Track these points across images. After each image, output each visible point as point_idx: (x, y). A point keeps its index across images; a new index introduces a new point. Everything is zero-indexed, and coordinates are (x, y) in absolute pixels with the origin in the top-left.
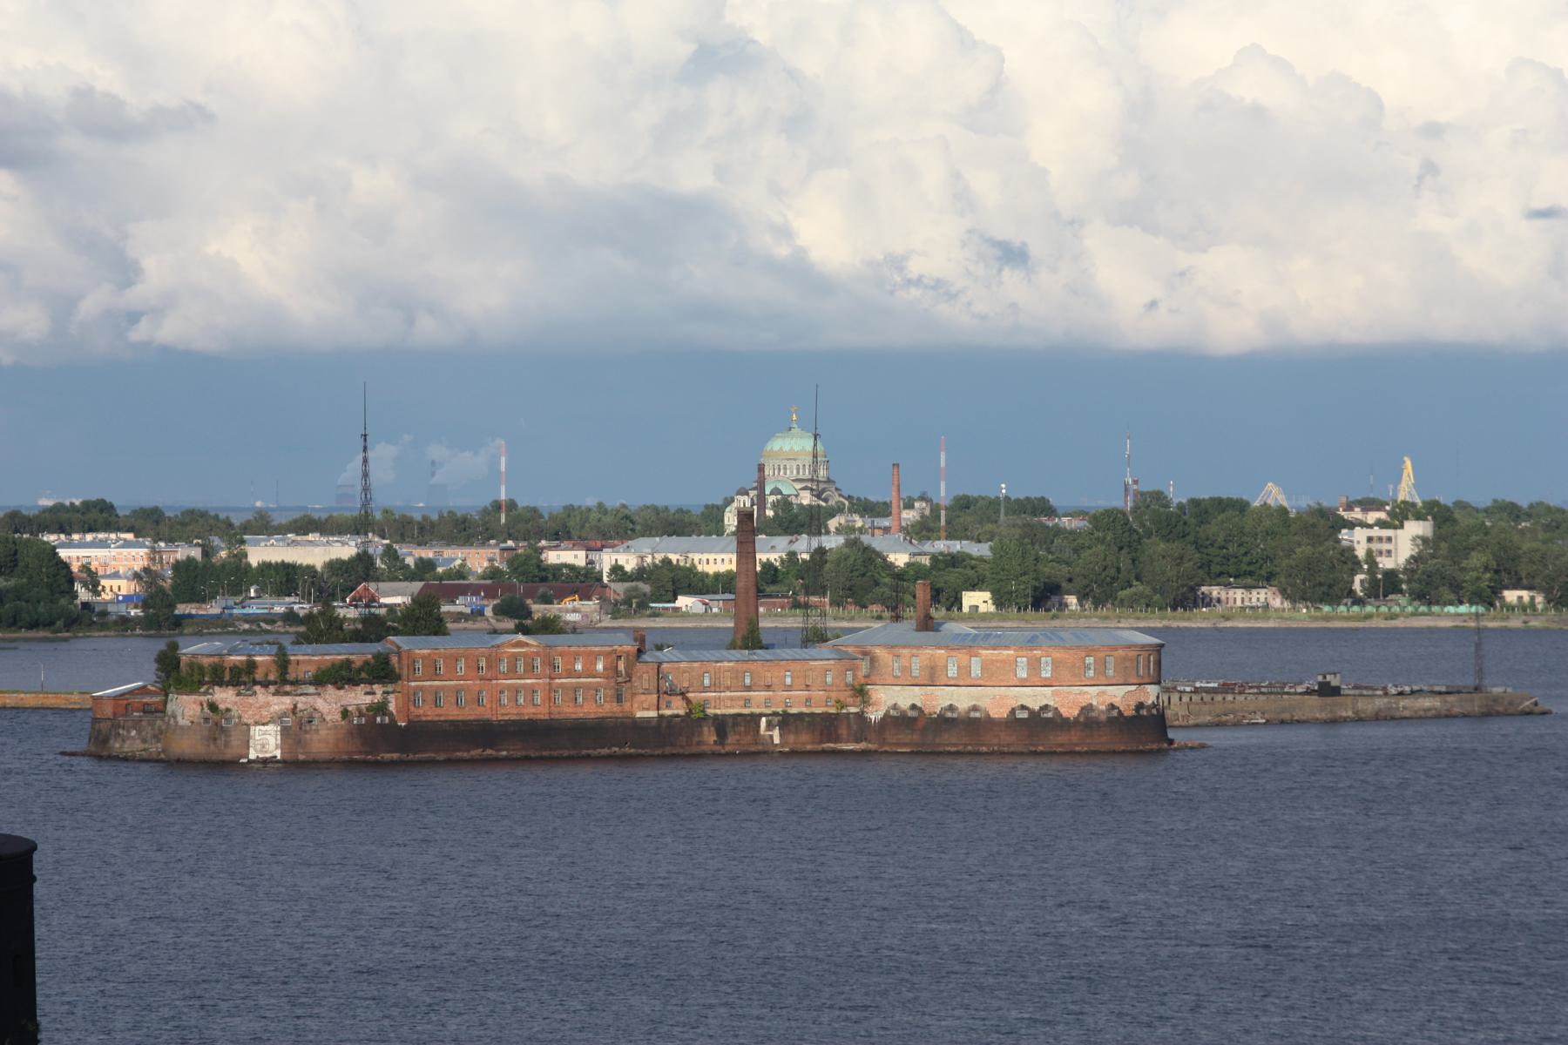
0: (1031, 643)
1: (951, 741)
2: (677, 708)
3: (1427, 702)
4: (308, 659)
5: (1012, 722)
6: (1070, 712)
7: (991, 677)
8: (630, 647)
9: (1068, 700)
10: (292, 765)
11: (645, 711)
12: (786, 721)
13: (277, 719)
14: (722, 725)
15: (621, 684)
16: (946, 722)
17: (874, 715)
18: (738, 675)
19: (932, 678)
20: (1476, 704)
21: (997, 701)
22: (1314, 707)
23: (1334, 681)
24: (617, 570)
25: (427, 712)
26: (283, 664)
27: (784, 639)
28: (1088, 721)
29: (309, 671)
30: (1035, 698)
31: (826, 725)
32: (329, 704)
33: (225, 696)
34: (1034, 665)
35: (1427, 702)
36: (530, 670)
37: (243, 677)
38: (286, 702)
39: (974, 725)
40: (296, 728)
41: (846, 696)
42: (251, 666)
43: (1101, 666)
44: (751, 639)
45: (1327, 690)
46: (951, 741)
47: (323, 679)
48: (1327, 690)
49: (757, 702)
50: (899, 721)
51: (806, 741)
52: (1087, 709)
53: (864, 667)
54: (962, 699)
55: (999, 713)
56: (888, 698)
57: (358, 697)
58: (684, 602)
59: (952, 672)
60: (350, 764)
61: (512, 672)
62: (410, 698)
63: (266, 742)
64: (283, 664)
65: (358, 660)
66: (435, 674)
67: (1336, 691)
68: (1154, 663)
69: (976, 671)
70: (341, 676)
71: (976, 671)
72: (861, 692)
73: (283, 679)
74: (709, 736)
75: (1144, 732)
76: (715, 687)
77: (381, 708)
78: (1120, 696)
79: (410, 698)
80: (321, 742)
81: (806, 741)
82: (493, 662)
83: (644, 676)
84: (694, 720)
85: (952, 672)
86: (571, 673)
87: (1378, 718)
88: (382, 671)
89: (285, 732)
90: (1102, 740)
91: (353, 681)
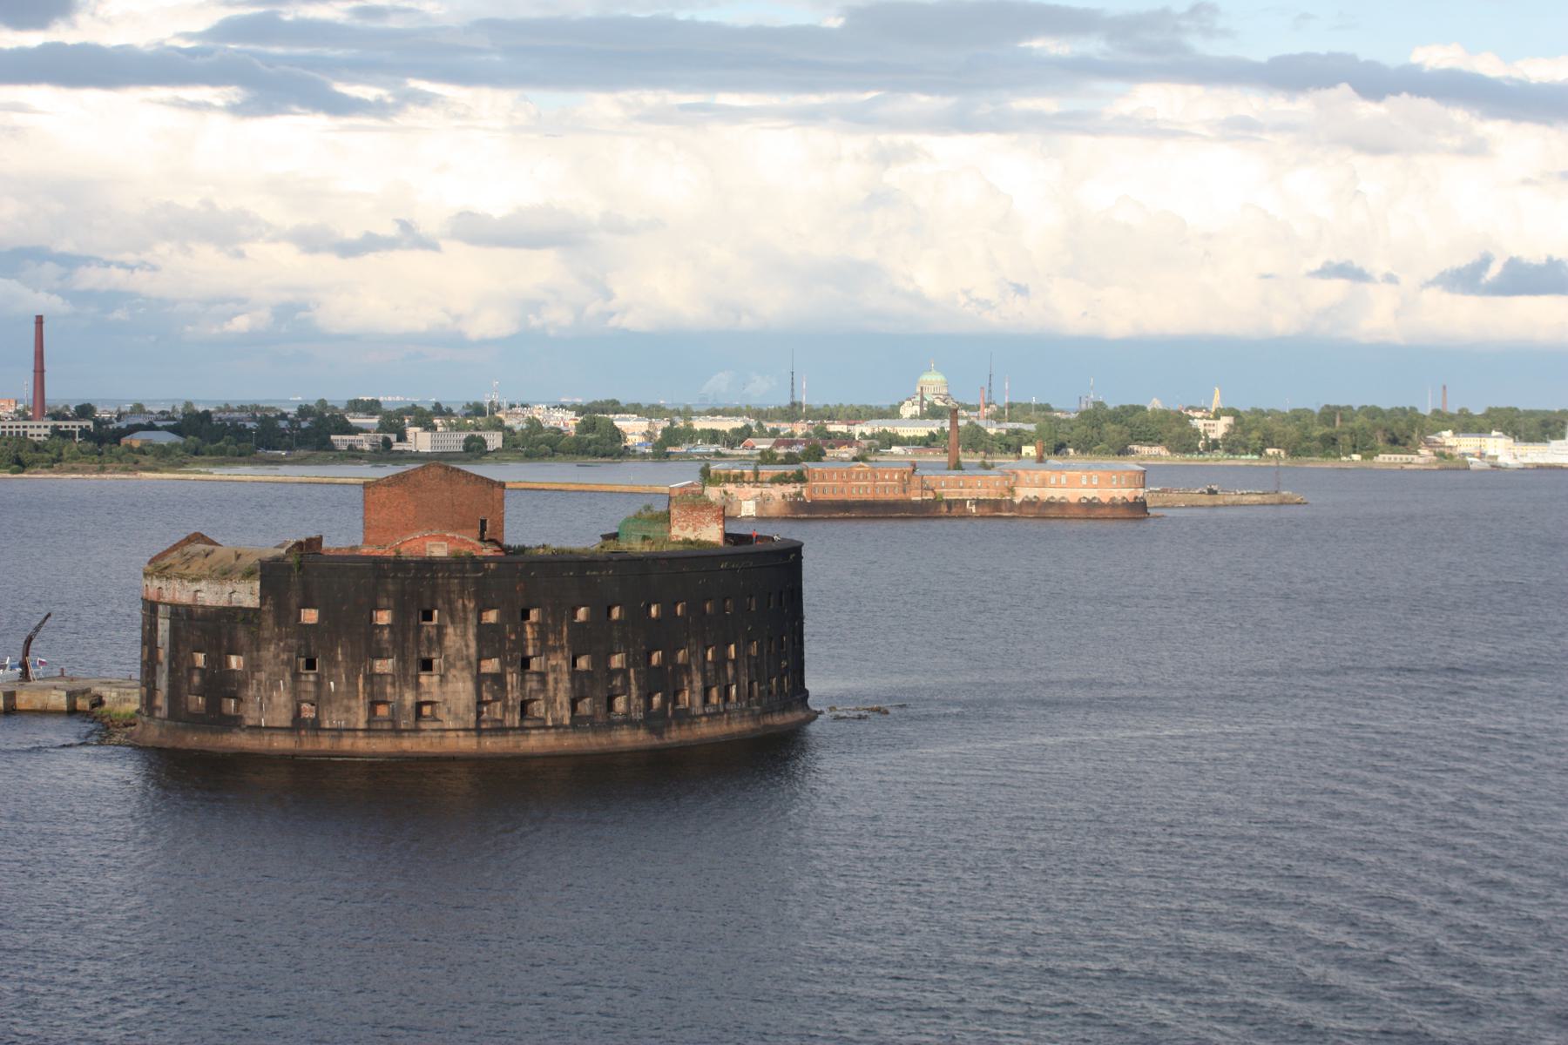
0: (1088, 469)
1: (1051, 512)
2: (930, 496)
3: (1254, 498)
4: (767, 471)
5: (1079, 504)
6: (1105, 500)
7: (1071, 483)
8: (910, 469)
9: (1105, 494)
10: (760, 519)
11: (916, 497)
12: (978, 503)
13: (754, 498)
14: (950, 504)
15: (905, 485)
16: (1050, 504)
17: (1017, 500)
18: (957, 481)
19: (1044, 484)
20: (1276, 499)
21: (1072, 495)
22: (1206, 500)
23: (1215, 488)
24: (862, 434)
25: (820, 496)
26: (757, 474)
27: (972, 466)
28: (1113, 505)
29: (768, 478)
30: (1090, 494)
31: (996, 505)
32: (777, 492)
33: (730, 488)
34: (1090, 479)
35: (1254, 498)
36: (865, 478)
37: (738, 479)
38: (758, 491)
39: (1062, 505)
40: (762, 502)
41: (1005, 492)
42: (743, 475)
43: (1119, 480)
44: (958, 466)
45: (1212, 492)
46: (1051, 512)
47: (773, 481)
48: (1212, 492)
49: (966, 494)
50: (1029, 503)
51: (987, 511)
52: (1113, 499)
53: (1013, 479)
54: (1056, 494)
55: (1074, 500)
56: (1023, 493)
57: (790, 489)
58: (895, 449)
59: (1053, 481)
60: (786, 518)
61: (857, 479)
62: (812, 490)
63: (749, 509)
64: (757, 474)
65: (789, 473)
66: (823, 479)
67: (1215, 493)
68: (1143, 478)
69: (1064, 481)
70: (781, 480)
71: (1064, 481)
72: (1011, 490)
73: (757, 480)
74: (944, 509)
75: (1138, 509)
76: (947, 486)
77: (799, 494)
78: (1127, 493)
79: (812, 490)
80: (774, 509)
81: (987, 511)
82: (849, 474)
83: (916, 482)
84: (937, 502)
85: (1053, 481)
86: (883, 480)
87: (1234, 505)
88: (800, 478)
89: (757, 504)
90: (1119, 513)
91: (787, 482)
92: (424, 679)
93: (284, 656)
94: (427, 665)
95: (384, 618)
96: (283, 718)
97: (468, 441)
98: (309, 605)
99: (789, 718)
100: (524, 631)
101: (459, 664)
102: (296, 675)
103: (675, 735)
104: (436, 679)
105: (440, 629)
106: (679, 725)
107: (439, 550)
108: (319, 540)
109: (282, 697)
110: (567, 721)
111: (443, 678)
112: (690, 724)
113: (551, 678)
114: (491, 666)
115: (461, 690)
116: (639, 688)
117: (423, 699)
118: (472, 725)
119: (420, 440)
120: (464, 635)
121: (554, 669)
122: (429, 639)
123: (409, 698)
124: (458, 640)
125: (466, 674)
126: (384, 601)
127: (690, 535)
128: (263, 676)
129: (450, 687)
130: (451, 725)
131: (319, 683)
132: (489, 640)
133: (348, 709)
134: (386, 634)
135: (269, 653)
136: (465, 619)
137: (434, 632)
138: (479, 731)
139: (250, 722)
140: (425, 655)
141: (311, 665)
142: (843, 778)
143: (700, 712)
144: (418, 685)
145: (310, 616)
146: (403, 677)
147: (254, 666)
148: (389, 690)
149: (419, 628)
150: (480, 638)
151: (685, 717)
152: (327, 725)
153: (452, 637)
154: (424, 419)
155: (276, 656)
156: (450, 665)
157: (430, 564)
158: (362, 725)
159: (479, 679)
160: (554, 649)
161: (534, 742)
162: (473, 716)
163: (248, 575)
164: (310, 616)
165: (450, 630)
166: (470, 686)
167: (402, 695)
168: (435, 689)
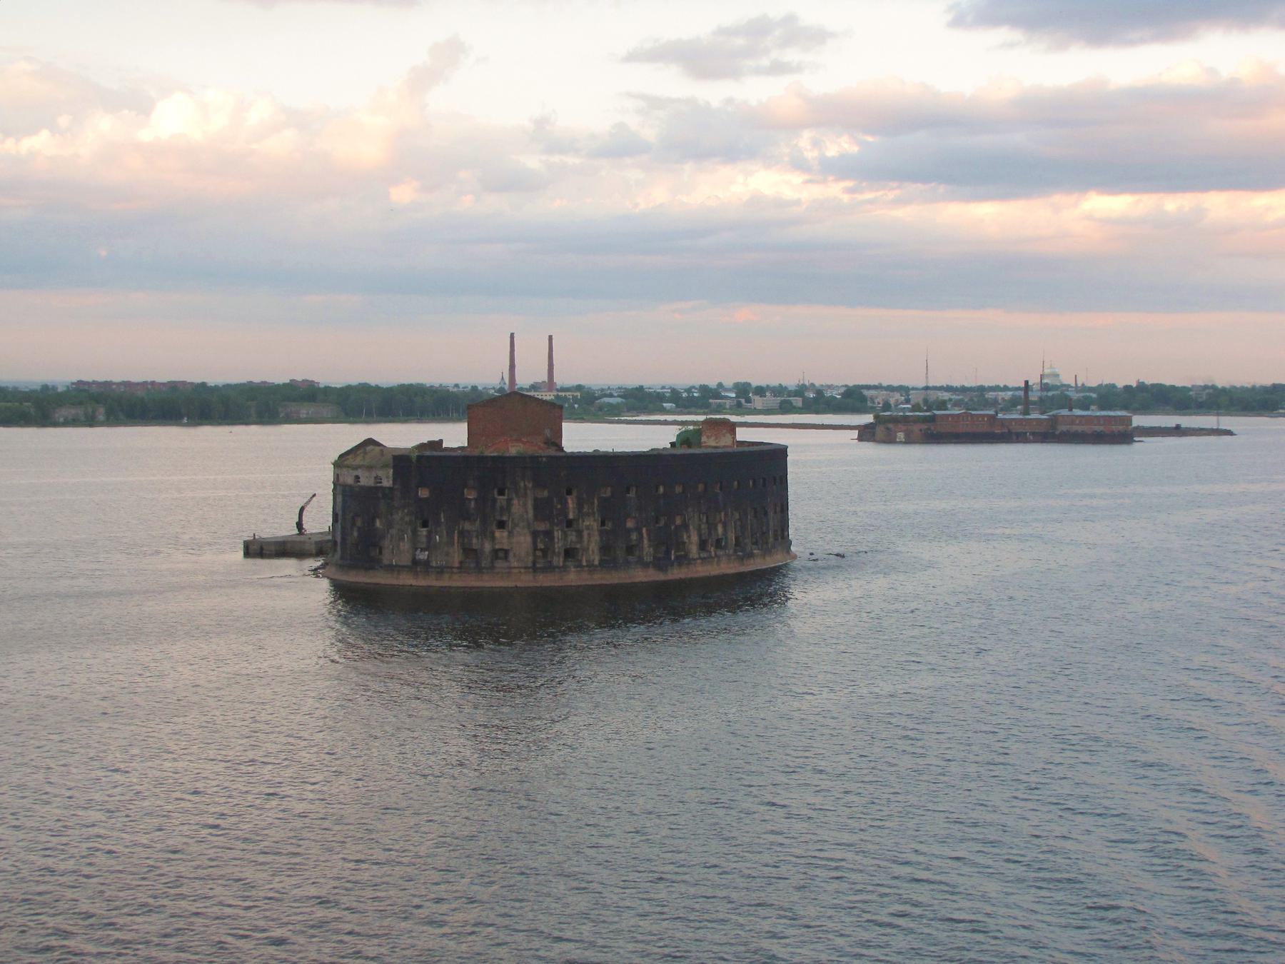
92: (497, 534)
93: (407, 519)
94: (501, 525)
95: (471, 495)
96: (406, 560)
97: (782, 403)
98: (422, 484)
99: (769, 562)
100: (566, 502)
101: (521, 524)
102: (414, 532)
103: (676, 574)
104: (505, 534)
105: (509, 501)
106: (680, 565)
107: (513, 450)
108: (441, 441)
109: (405, 545)
110: (596, 563)
111: (511, 534)
112: (689, 564)
113: (585, 533)
114: (542, 527)
115: (522, 542)
116: (649, 540)
117: (497, 547)
118: (530, 564)
119: (758, 402)
120: (525, 505)
121: (588, 528)
122: (502, 508)
123: (488, 547)
124: (521, 508)
125: (526, 531)
126: (471, 482)
127: (712, 442)
128: (394, 531)
129: (514, 540)
130: (516, 564)
131: (429, 536)
132: (542, 509)
133: (447, 554)
134: (473, 503)
135: (397, 516)
136: (525, 495)
137: (504, 503)
138: (534, 569)
139: (386, 562)
140: (498, 518)
141: (425, 525)
142: (811, 602)
143: (696, 556)
144: (493, 538)
145: (424, 493)
146: (485, 533)
147: (390, 525)
148: (474, 541)
149: (494, 501)
150: (536, 508)
151: (684, 560)
152: (434, 564)
153: (516, 507)
154: (760, 391)
155: (402, 519)
156: (516, 525)
157: (501, 461)
158: (457, 565)
159: (535, 534)
160: (588, 515)
161: (573, 578)
162: (531, 558)
163: (385, 466)
164: (424, 493)
165: (515, 502)
166: (529, 539)
167: (482, 545)
168: (505, 541)
